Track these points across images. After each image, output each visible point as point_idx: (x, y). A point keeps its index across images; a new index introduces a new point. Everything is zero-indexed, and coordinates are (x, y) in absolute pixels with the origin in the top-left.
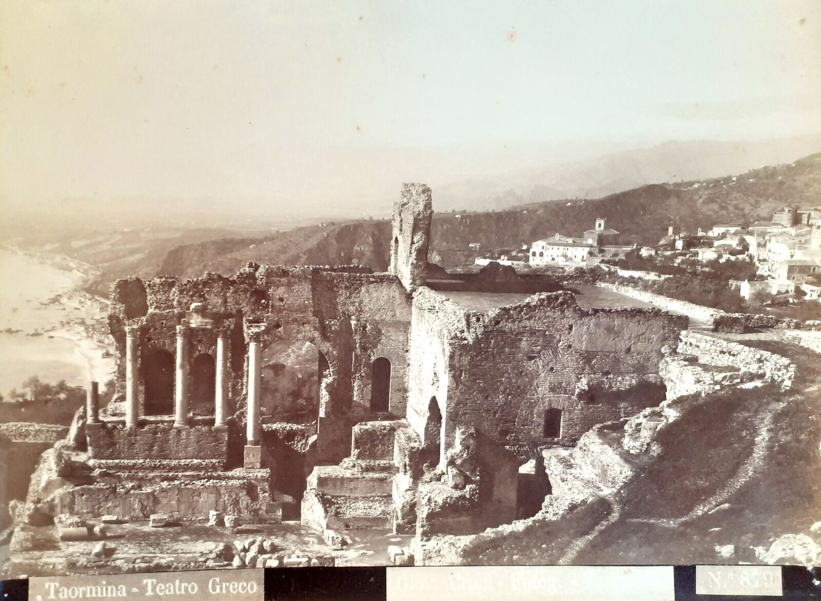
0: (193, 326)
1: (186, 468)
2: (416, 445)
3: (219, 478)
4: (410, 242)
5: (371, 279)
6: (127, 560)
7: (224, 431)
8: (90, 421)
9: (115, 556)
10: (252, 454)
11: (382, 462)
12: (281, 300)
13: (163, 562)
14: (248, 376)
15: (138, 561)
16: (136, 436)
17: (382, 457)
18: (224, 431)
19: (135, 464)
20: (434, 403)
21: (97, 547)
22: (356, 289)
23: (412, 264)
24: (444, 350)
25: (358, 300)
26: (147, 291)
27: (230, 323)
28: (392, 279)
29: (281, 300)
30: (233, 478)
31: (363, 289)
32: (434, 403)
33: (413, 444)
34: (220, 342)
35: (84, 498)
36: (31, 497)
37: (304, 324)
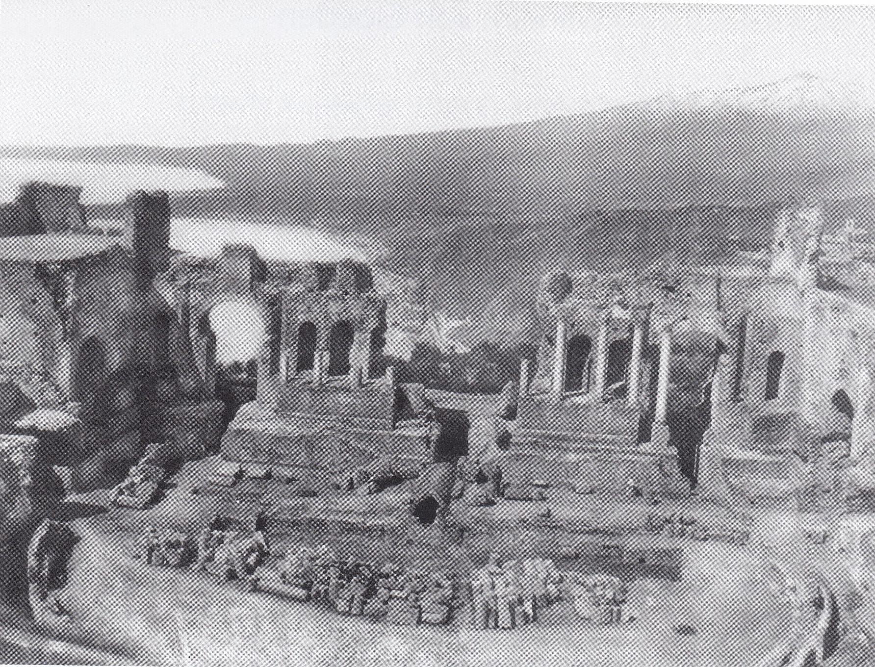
1: (604, 441)
5: (771, 281)
7: (636, 411)
10: (660, 432)
11: (779, 447)
18: (636, 411)
19: (559, 436)
27: (642, 314)
31: (762, 288)
33: (813, 432)
35: (518, 462)
36: (473, 458)
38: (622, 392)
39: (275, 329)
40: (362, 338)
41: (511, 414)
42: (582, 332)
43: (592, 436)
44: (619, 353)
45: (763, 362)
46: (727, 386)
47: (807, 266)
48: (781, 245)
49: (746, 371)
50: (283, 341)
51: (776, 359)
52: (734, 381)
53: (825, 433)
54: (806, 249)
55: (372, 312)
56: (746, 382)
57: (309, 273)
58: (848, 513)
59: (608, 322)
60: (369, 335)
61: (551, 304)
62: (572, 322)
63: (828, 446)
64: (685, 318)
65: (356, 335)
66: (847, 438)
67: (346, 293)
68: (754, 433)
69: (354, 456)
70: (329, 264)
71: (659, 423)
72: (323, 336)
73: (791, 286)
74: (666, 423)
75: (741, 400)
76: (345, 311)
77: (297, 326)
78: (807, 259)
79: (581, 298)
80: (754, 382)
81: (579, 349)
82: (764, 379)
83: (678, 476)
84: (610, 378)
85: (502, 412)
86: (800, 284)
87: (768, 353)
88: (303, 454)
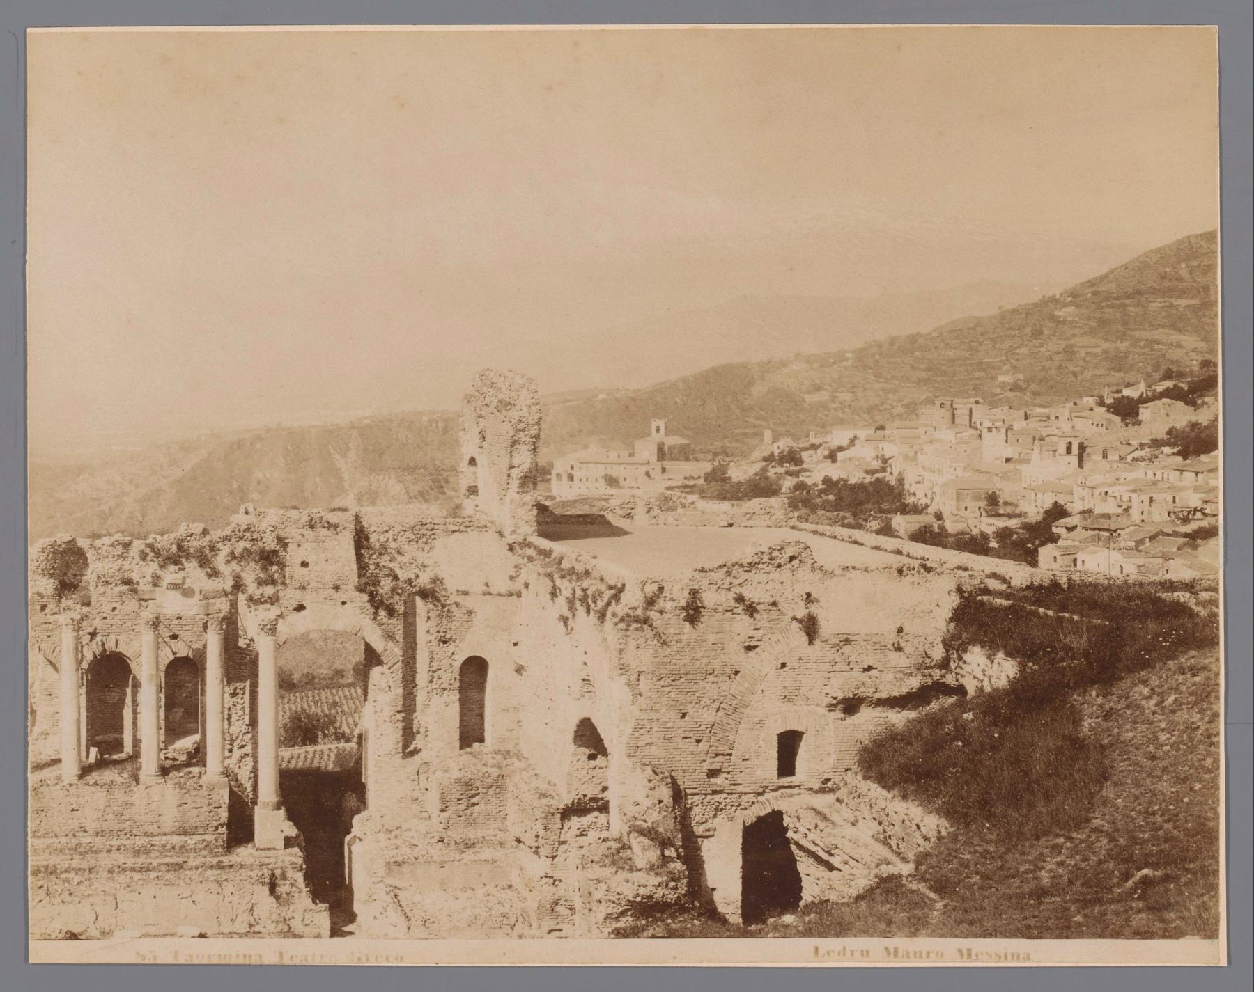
3: (220, 866)
5: (452, 528)
10: (272, 825)
12: (304, 564)
20: (589, 738)
24: (604, 640)
29: (304, 564)
31: (438, 543)
38: (197, 756)
42: (111, 646)
43: (141, 841)
48: (472, 461)
52: (400, 716)
53: (566, 799)
54: (512, 467)
56: (422, 718)
59: (156, 624)
62: (91, 630)
63: (575, 822)
64: (300, 608)
66: (604, 808)
73: (490, 536)
78: (515, 484)
81: (108, 676)
82: (456, 708)
84: (174, 731)
86: (507, 532)
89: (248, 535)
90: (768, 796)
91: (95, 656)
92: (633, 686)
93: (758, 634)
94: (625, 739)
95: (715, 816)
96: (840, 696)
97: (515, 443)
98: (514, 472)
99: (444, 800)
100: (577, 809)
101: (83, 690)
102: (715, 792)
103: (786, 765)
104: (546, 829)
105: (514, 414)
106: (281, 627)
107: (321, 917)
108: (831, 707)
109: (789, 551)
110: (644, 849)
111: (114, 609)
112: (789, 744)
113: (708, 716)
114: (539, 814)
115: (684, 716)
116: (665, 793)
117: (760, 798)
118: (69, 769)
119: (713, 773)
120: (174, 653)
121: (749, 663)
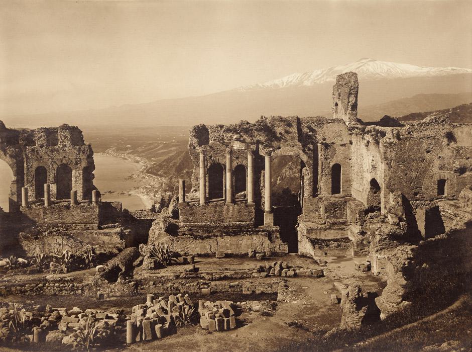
0: (235, 148)
2: (362, 207)
4: (346, 102)
5: (329, 121)
6: (208, 274)
8: (181, 201)
9: (200, 272)
10: (268, 220)
11: (341, 220)
13: (228, 274)
14: (264, 176)
15: (214, 274)
16: (205, 209)
17: (341, 217)
18: (252, 206)
21: (190, 267)
22: (321, 126)
23: (349, 113)
25: (322, 132)
26: (209, 131)
27: (253, 147)
28: (340, 121)
30: (259, 231)
31: (325, 126)
32: (374, 183)
33: (360, 207)
34: (250, 158)
35: (179, 243)
36: (150, 243)
37: (293, 146)
39: (19, 173)
40: (77, 174)
41: (175, 214)
44: (239, 173)
45: (327, 171)
46: (308, 187)
47: (350, 112)
49: (319, 177)
50: (25, 180)
51: (336, 170)
52: (312, 183)
54: (349, 102)
55: (83, 157)
57: (40, 135)
58: (381, 250)
59: (231, 152)
60: (82, 171)
61: (196, 145)
64: (279, 148)
65: (73, 172)
67: (66, 146)
68: (326, 213)
69: (71, 248)
70: (54, 129)
71: (267, 212)
72: (51, 176)
73: (341, 124)
74: (270, 212)
75: (317, 195)
76: (65, 157)
77: (34, 169)
78: (350, 108)
79: (214, 140)
80: (324, 184)
81: (215, 172)
83: (280, 242)
85: (170, 215)
87: (332, 164)
88: (38, 249)
89: (262, 124)
90: (435, 201)
91: (211, 164)
92: (389, 165)
93: (431, 147)
94: (386, 182)
95: (417, 208)
96: (459, 167)
97: (350, 94)
98: (350, 104)
99: (326, 209)
100: (371, 209)
101: (207, 176)
102: (416, 200)
103: (441, 191)
104: (360, 216)
105: (350, 84)
106: (272, 154)
107: (285, 248)
108: (455, 171)
109: (442, 119)
110: (392, 218)
111: (218, 148)
112: (441, 183)
113: (414, 174)
114: (357, 212)
115: (406, 174)
116: (400, 199)
117: (432, 202)
118: (202, 201)
119: (416, 194)
120: (237, 163)
121: (428, 156)
